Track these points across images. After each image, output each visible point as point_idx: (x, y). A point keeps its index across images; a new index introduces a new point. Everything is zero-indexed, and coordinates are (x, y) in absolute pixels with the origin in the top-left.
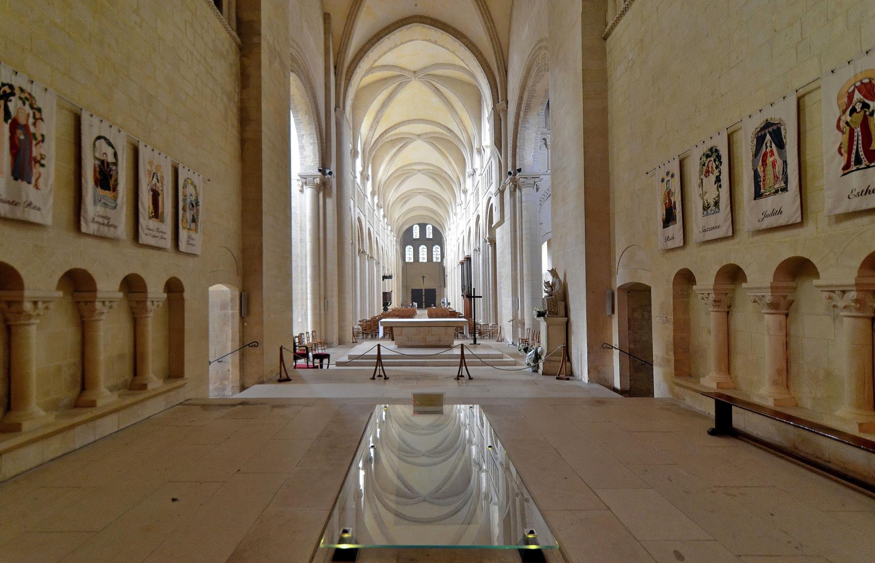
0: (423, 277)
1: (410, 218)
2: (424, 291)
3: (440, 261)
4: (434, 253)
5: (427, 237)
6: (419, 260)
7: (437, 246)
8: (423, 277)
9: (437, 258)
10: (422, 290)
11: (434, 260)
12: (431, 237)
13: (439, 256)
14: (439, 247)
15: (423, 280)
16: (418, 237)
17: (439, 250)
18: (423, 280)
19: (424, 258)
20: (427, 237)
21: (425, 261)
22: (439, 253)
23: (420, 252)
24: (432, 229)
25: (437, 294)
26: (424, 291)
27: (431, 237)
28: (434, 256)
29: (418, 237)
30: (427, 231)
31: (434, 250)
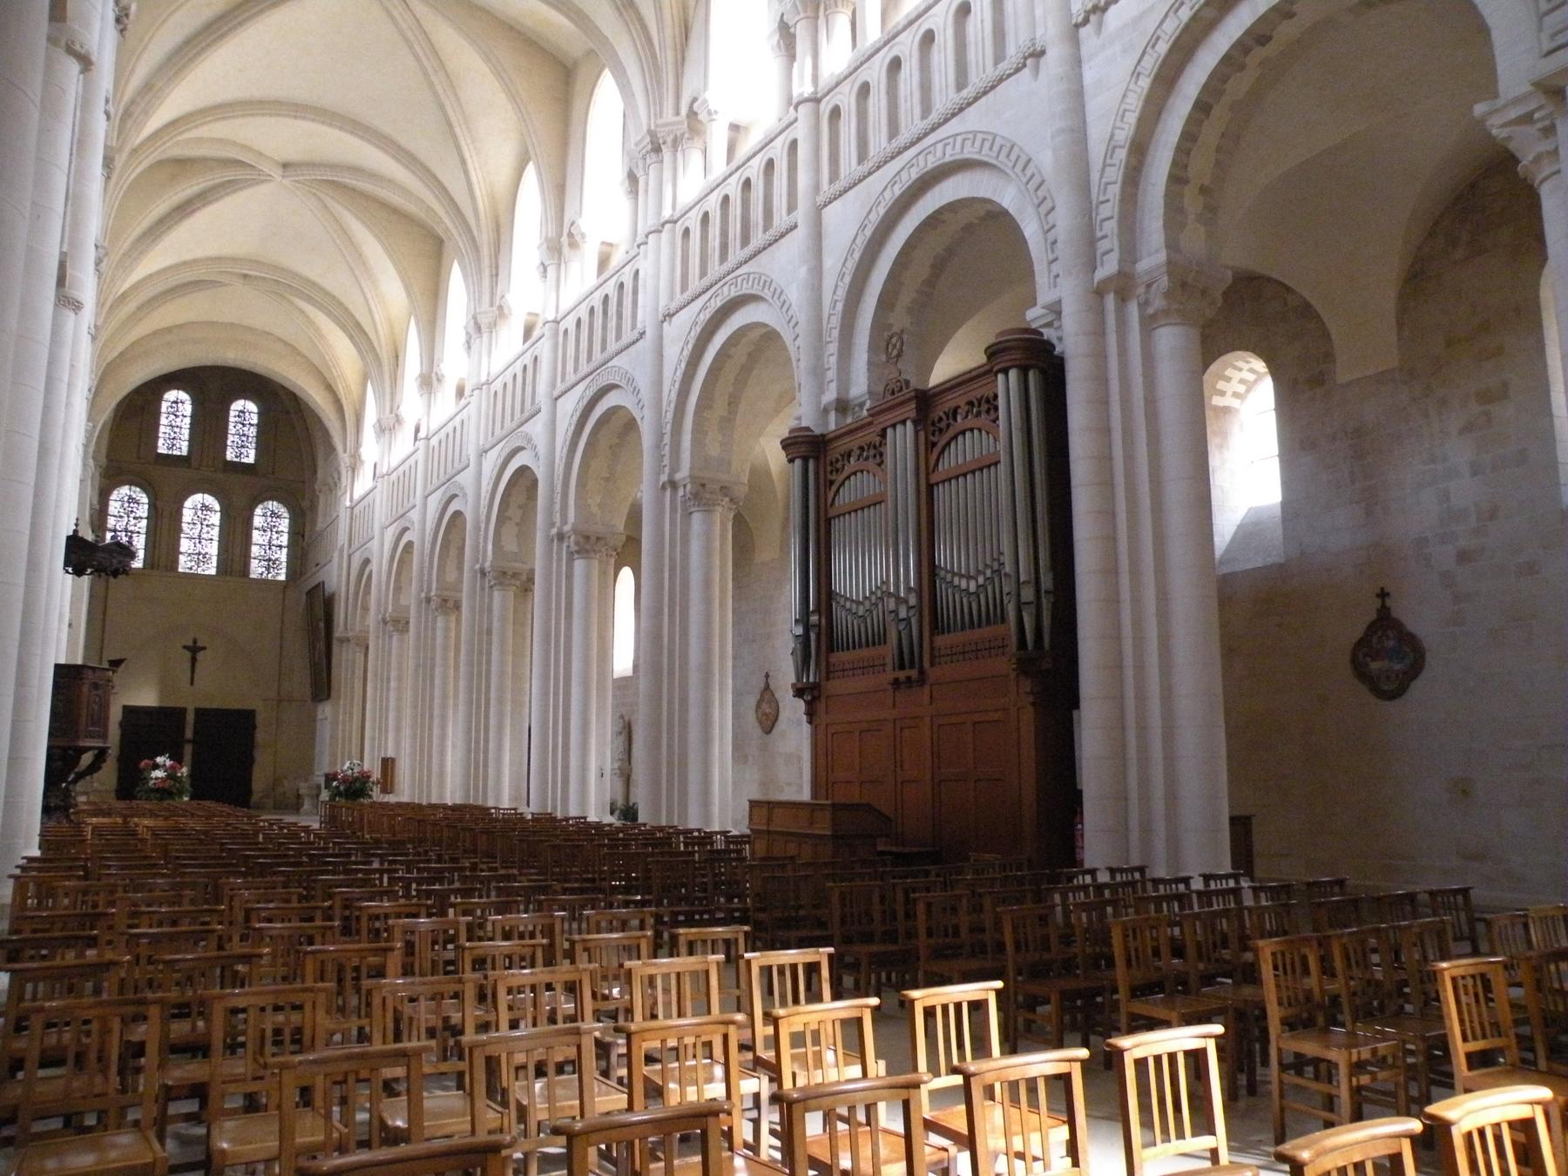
0: (194, 650)
1: (169, 330)
2: (190, 717)
3: (282, 577)
4: (256, 536)
5: (230, 455)
6: (175, 563)
7: (273, 505)
8: (194, 650)
9: (271, 563)
10: (183, 711)
11: (256, 569)
12: (250, 457)
13: (283, 555)
14: (283, 511)
15: (194, 661)
16: (183, 448)
17: (284, 525)
18: (194, 661)
19: (202, 557)
20: (230, 455)
21: (211, 569)
22: (284, 539)
23: (185, 526)
24: (255, 420)
25: (260, 736)
26: (190, 717)
27: (250, 457)
28: (255, 550)
29: (183, 448)
30: (232, 430)
31: (258, 521)
